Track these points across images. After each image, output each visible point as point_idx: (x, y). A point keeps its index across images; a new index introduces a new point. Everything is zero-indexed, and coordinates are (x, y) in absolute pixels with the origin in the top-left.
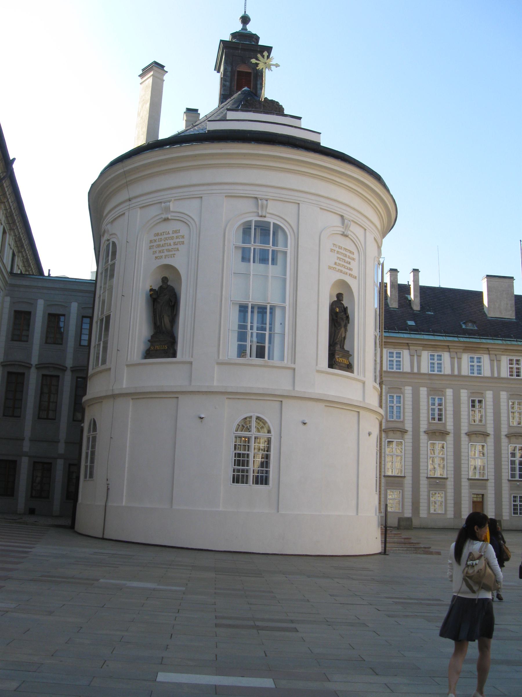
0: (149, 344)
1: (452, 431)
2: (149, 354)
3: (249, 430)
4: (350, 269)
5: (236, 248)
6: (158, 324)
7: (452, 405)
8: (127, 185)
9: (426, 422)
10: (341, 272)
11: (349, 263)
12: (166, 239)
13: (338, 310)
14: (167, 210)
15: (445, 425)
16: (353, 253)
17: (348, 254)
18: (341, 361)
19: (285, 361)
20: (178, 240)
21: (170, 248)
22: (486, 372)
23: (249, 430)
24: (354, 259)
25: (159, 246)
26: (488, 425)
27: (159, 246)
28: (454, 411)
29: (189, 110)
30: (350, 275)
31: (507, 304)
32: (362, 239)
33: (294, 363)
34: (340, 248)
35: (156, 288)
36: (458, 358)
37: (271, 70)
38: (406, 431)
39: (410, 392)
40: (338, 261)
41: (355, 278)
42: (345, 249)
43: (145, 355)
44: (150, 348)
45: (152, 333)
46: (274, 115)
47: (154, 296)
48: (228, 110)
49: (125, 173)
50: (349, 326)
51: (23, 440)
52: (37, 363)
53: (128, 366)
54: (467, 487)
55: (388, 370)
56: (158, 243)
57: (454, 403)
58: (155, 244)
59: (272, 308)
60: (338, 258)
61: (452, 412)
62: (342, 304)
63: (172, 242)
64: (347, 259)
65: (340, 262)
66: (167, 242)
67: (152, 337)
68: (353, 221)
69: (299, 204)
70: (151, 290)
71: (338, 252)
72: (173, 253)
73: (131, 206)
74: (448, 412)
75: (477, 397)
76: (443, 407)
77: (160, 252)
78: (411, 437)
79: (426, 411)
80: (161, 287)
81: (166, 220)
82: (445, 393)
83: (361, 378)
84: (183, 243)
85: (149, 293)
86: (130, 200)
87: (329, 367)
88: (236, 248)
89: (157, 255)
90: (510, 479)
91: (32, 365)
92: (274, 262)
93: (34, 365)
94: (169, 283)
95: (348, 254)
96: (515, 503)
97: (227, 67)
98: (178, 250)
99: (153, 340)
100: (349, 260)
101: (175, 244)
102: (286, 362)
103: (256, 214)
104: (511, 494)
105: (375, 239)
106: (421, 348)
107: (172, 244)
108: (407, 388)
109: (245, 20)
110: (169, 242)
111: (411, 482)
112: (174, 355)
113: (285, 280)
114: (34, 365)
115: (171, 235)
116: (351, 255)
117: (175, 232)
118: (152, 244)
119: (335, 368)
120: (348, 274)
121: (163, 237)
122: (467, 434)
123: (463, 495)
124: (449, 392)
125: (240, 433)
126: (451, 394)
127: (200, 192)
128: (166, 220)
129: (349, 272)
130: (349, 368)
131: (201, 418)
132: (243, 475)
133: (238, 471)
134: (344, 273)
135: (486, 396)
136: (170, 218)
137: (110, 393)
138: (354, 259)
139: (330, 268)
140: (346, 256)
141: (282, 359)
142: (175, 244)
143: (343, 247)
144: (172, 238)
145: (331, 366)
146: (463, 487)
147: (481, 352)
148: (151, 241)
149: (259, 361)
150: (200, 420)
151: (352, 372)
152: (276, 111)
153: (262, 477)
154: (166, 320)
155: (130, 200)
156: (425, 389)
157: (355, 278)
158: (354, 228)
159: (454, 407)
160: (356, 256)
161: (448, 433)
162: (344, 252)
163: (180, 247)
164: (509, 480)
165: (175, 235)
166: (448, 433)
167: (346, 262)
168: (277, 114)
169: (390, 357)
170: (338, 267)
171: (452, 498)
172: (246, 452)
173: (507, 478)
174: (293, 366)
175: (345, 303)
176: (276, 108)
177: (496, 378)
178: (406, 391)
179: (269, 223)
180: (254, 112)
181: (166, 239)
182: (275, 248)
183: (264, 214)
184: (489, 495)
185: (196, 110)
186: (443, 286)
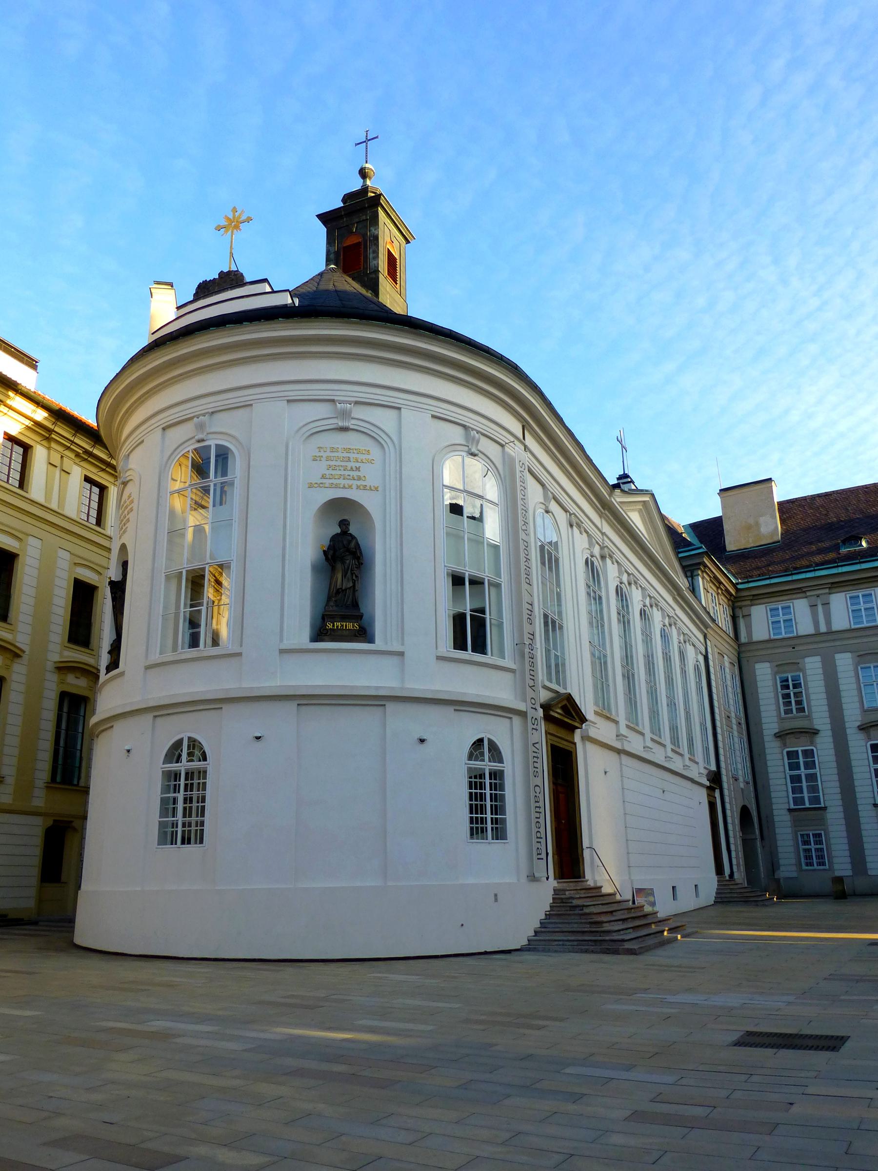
4: (359, 478)
10: (337, 486)
11: (358, 469)
18: (337, 627)
23: (178, 760)
24: (371, 462)
30: (358, 487)
33: (241, 646)
34: (333, 450)
37: (240, 230)
40: (327, 472)
41: (376, 489)
42: (348, 450)
46: (228, 290)
60: (330, 466)
62: (351, 535)
64: (349, 465)
65: (334, 472)
68: (356, 403)
71: (328, 459)
83: (396, 647)
95: (352, 455)
97: (330, 248)
100: (358, 465)
103: (193, 441)
105: (433, 417)
120: (354, 487)
129: (355, 483)
130: (364, 634)
131: (128, 751)
134: (344, 487)
138: (371, 462)
139: (311, 486)
143: (340, 447)
149: (193, 653)
151: (371, 640)
157: (376, 489)
162: (348, 455)
163: (131, 515)
167: (349, 468)
170: (327, 482)
174: (237, 650)
176: (233, 280)
179: (209, 447)
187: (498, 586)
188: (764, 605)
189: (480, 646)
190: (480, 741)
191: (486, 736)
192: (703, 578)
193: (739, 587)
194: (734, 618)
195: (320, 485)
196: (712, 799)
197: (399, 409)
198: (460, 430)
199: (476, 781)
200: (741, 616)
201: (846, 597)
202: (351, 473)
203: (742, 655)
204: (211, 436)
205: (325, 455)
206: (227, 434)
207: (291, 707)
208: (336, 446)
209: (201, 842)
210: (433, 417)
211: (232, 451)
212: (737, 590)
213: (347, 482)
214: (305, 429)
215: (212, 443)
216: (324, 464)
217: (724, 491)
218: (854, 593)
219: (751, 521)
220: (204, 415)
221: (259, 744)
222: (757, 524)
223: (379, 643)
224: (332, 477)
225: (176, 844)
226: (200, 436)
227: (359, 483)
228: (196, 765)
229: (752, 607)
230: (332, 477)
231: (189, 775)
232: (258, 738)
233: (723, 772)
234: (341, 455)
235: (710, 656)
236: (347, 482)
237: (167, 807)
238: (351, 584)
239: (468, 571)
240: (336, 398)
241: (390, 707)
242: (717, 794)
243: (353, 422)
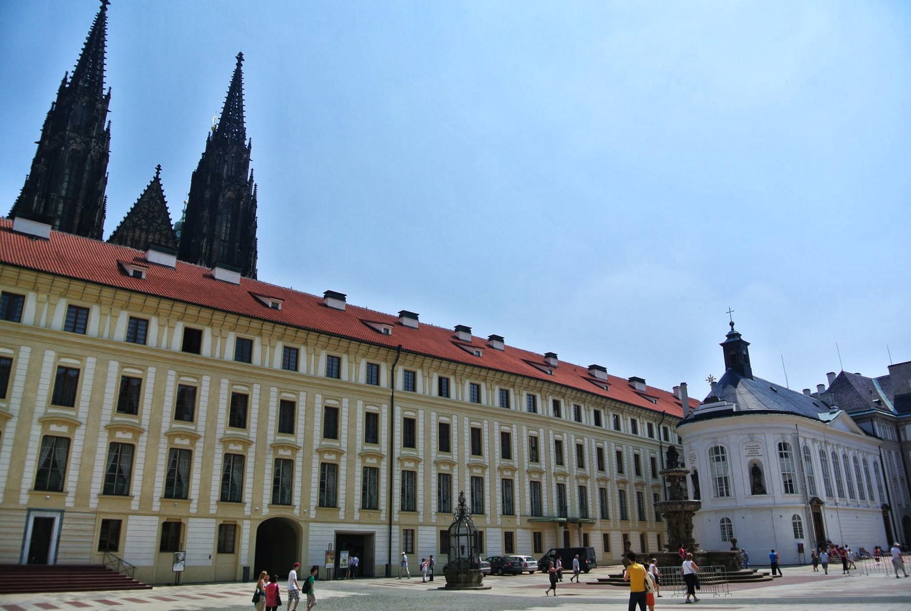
23: (723, 522)
32: (763, 439)
84: (696, 458)
95: (755, 447)
109: (732, 324)
125: (722, 524)
130: (764, 492)
139: (746, 456)
140: (754, 448)
145: (753, 494)
160: (760, 446)
163: (696, 459)
175: (758, 466)
189: (792, 492)
190: (795, 515)
192: (877, 421)
195: (748, 456)
196: (886, 515)
199: (794, 524)
215: (719, 445)
217: (889, 367)
221: (743, 519)
224: (751, 453)
228: (730, 524)
230: (751, 453)
233: (892, 503)
235: (883, 455)
242: (889, 513)
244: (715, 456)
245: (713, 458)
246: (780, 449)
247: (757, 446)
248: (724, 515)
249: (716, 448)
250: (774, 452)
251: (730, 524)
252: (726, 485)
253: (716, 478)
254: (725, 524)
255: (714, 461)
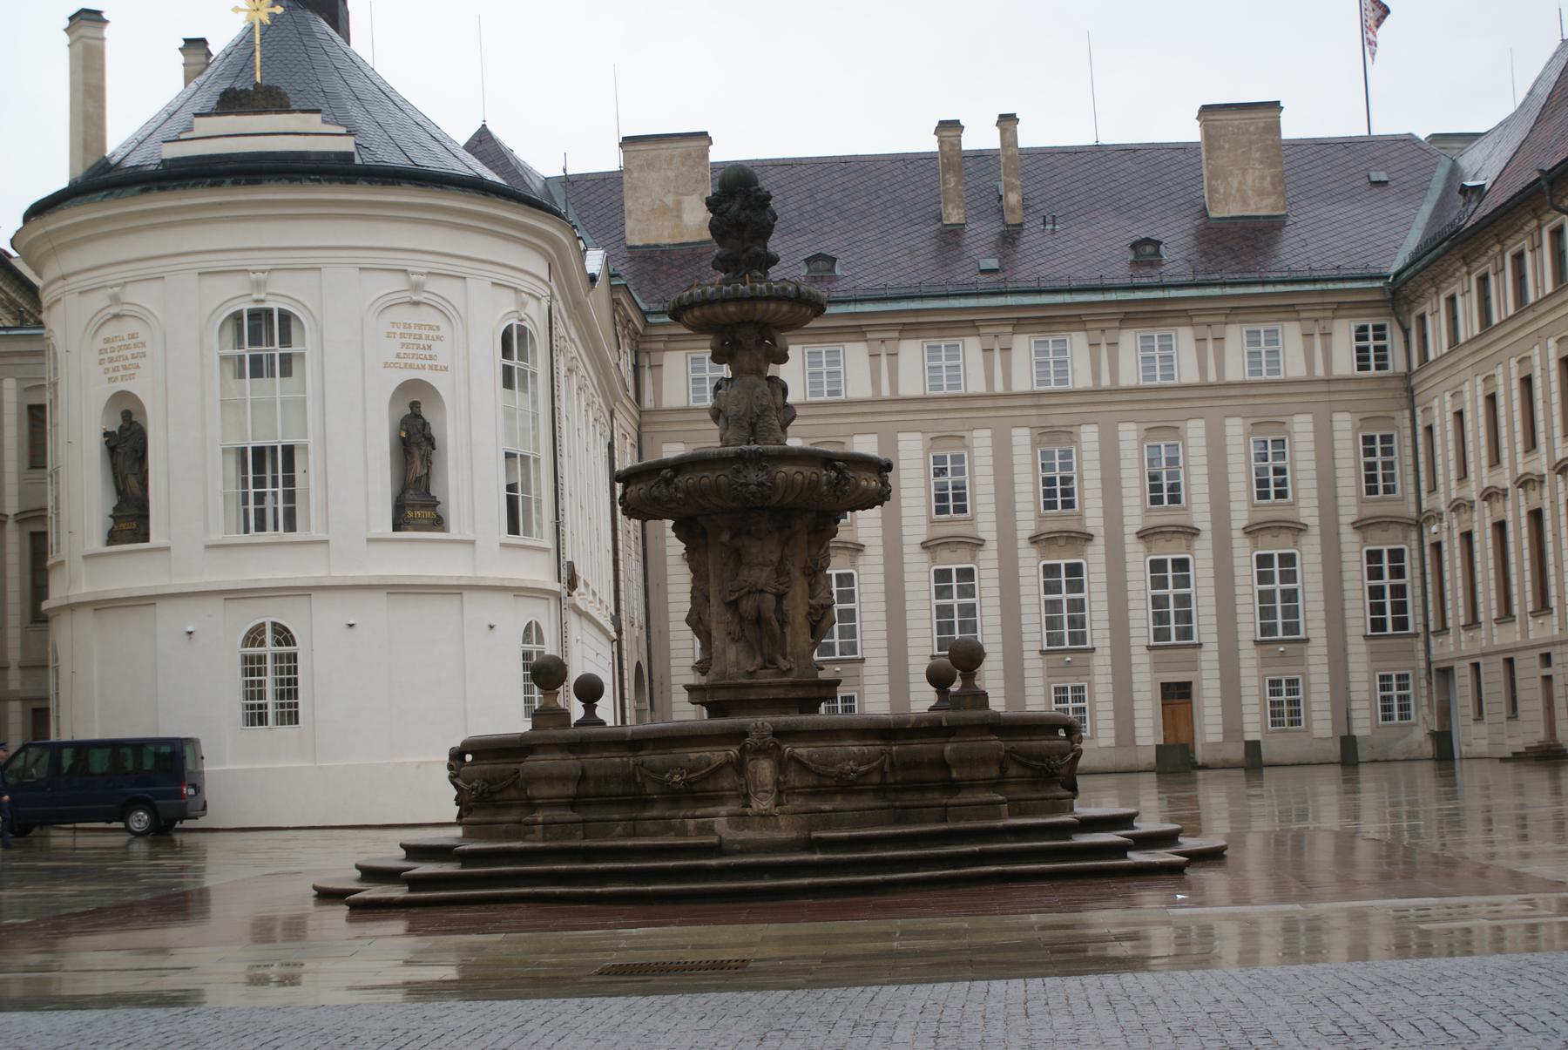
0: (111, 520)
1: (1102, 531)
2: (113, 538)
3: (262, 644)
4: (431, 358)
5: (223, 358)
6: (122, 488)
7: (1097, 465)
8: (55, 251)
9: (1032, 515)
10: (411, 366)
12: (120, 348)
13: (404, 435)
14: (115, 299)
15: (1080, 517)
16: (438, 327)
17: (424, 332)
19: (313, 533)
20: (137, 350)
21: (127, 363)
22: (1187, 372)
23: (262, 644)
24: (439, 338)
25: (111, 360)
26: (1195, 508)
27: (111, 360)
28: (1102, 479)
29: (189, 43)
30: (431, 367)
31: (1263, 178)
33: (327, 531)
34: (406, 326)
35: (115, 429)
36: (1108, 344)
38: (980, 542)
39: (988, 442)
40: (404, 350)
42: (420, 326)
43: (107, 538)
44: (113, 528)
45: (114, 503)
47: (112, 444)
48: (196, 115)
49: (47, 234)
50: (435, 455)
51: (6, 668)
52: (16, 511)
53: (86, 557)
54: (1147, 668)
55: (928, 392)
56: (109, 355)
57: (1102, 459)
58: (105, 356)
59: (289, 451)
60: (403, 344)
61: (1098, 484)
62: (422, 418)
63: (128, 353)
64: (423, 342)
65: (407, 351)
66: (122, 353)
67: (115, 509)
69: (320, 269)
70: (106, 434)
72: (132, 371)
73: (67, 288)
74: (1086, 484)
75: (1165, 439)
76: (1074, 473)
77: (114, 370)
78: (995, 554)
79: (1030, 488)
80: (121, 428)
81: (117, 316)
82: (1079, 435)
83: (469, 536)
84: (144, 355)
85: (104, 440)
86: (64, 278)
87: (394, 530)
88: (223, 358)
89: (111, 375)
90: (1259, 638)
91: (6, 516)
92: (286, 371)
93: (11, 516)
94: (134, 419)
95: (424, 332)
96: (1292, 697)
98: (138, 367)
99: (117, 515)
100: (429, 342)
101: (134, 357)
102: (316, 534)
104: (1264, 676)
106: (1010, 329)
107: (129, 357)
108: (976, 433)
110: (124, 353)
111: (1000, 665)
112: (145, 537)
113: (304, 401)
114: (11, 516)
115: (126, 342)
116: (435, 333)
117: (132, 336)
118: (102, 356)
119: (405, 530)
120: (427, 367)
121: (115, 345)
122: (1141, 535)
123: (1135, 687)
124: (1089, 436)
126: (1095, 437)
127: (161, 269)
128: (117, 316)
129: (427, 363)
130: (439, 523)
131: (190, 633)
132: (260, 714)
133: (252, 707)
134: (418, 368)
135: (1186, 433)
136: (121, 313)
137: (65, 602)
139: (386, 365)
141: (308, 528)
142: (134, 357)
144: (128, 347)
145: (397, 527)
146: (1135, 669)
147: (1170, 321)
148: (101, 352)
150: (187, 637)
152: (274, 106)
153: (290, 713)
154: (133, 482)
155: (64, 278)
156: (1027, 431)
157: (446, 369)
158: (433, 285)
159: (1103, 469)
160: (445, 330)
161: (1089, 538)
164: (1257, 643)
165: (132, 342)
166: (1089, 538)
168: (277, 112)
169: (930, 358)
170: (403, 361)
171: (1109, 697)
172: (293, 676)
173: (1251, 636)
175: (426, 413)
177: (1211, 386)
178: (976, 443)
180: (238, 113)
181: (120, 348)
182: (286, 350)
183: (262, 296)
184: (1205, 684)
185: (202, 42)
186: (1106, 140)
187: (537, 461)
188: (683, 353)
191: (533, 619)
193: (651, 320)
194: (637, 369)
195: (395, 365)
197: (465, 278)
198: (511, 293)
200: (647, 365)
201: (803, 353)
202: (424, 352)
203: (645, 429)
204: (270, 297)
205: (399, 331)
206: (303, 305)
207: (382, 595)
208: (409, 322)
209: (297, 723)
210: (493, 283)
211: (297, 318)
212: (647, 325)
213: (420, 362)
214: (378, 303)
215: (274, 305)
216: (399, 341)
218: (815, 348)
219: (670, 200)
220: (263, 272)
222: (679, 204)
223: (454, 532)
224: (406, 356)
225: (266, 724)
226: (255, 296)
227: (431, 363)
228: (285, 649)
229: (666, 353)
230: (406, 356)
231: (278, 658)
232: (351, 625)
234: (411, 331)
236: (420, 362)
237: (254, 691)
238: (426, 471)
239: (519, 450)
240: (409, 269)
241: (467, 595)
243: (426, 295)
244: (247, 351)
245: (241, 358)
246: (506, 351)
247: (431, 328)
248: (268, 613)
249: (260, 318)
250: (491, 360)
251: (285, 649)
252: (290, 481)
253: (244, 450)
254: (269, 649)
255: (241, 375)
